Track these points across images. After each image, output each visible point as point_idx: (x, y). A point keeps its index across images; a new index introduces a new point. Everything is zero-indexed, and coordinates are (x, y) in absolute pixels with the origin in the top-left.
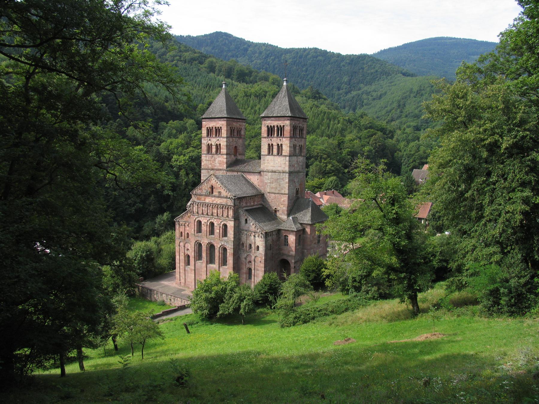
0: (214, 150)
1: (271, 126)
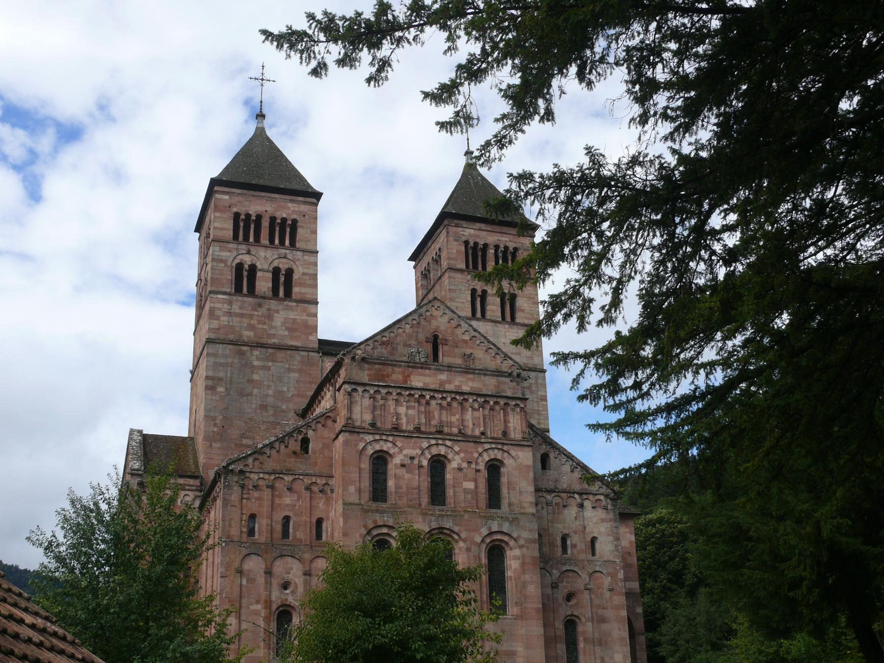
0: (264, 284)
1: (476, 244)
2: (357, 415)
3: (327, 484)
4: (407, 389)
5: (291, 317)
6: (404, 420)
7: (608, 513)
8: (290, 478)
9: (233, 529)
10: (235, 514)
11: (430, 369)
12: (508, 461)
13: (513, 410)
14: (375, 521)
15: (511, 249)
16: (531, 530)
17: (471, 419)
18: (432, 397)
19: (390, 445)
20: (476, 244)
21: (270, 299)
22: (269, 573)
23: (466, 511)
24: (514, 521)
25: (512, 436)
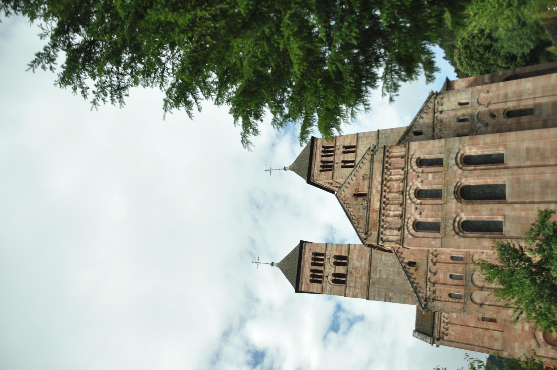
0: (341, 270)
1: (321, 166)
2: (395, 238)
3: (432, 253)
4: (380, 211)
5: (356, 257)
6: (397, 213)
7: (444, 97)
8: (429, 273)
9: (457, 307)
10: (449, 305)
11: (370, 198)
12: (417, 155)
13: (391, 153)
14: (451, 230)
15: (323, 149)
16: (454, 141)
17: (396, 175)
18: (385, 197)
19: (410, 221)
20: (321, 166)
21: (348, 268)
22: (482, 289)
23: (444, 179)
24: (449, 151)
25: (403, 153)
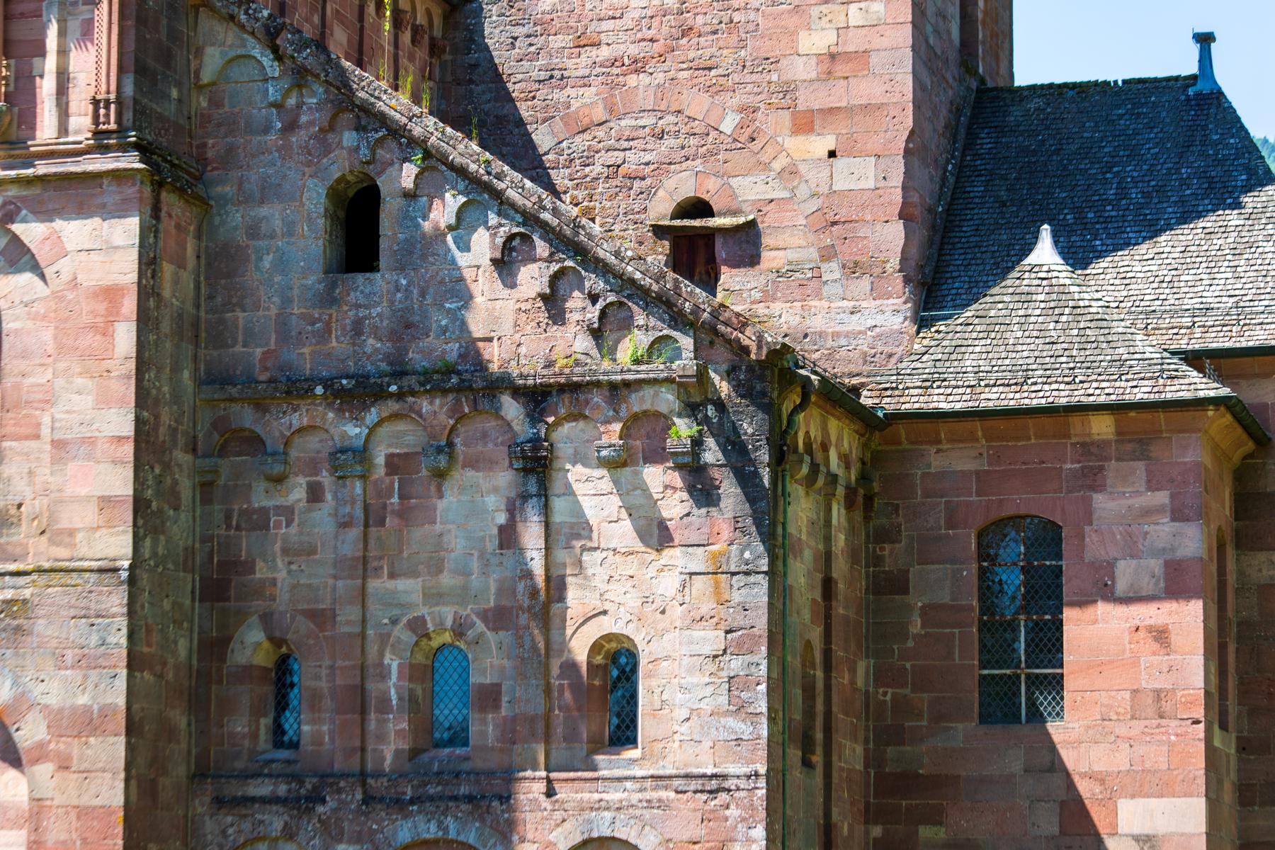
16: (85, 662)
